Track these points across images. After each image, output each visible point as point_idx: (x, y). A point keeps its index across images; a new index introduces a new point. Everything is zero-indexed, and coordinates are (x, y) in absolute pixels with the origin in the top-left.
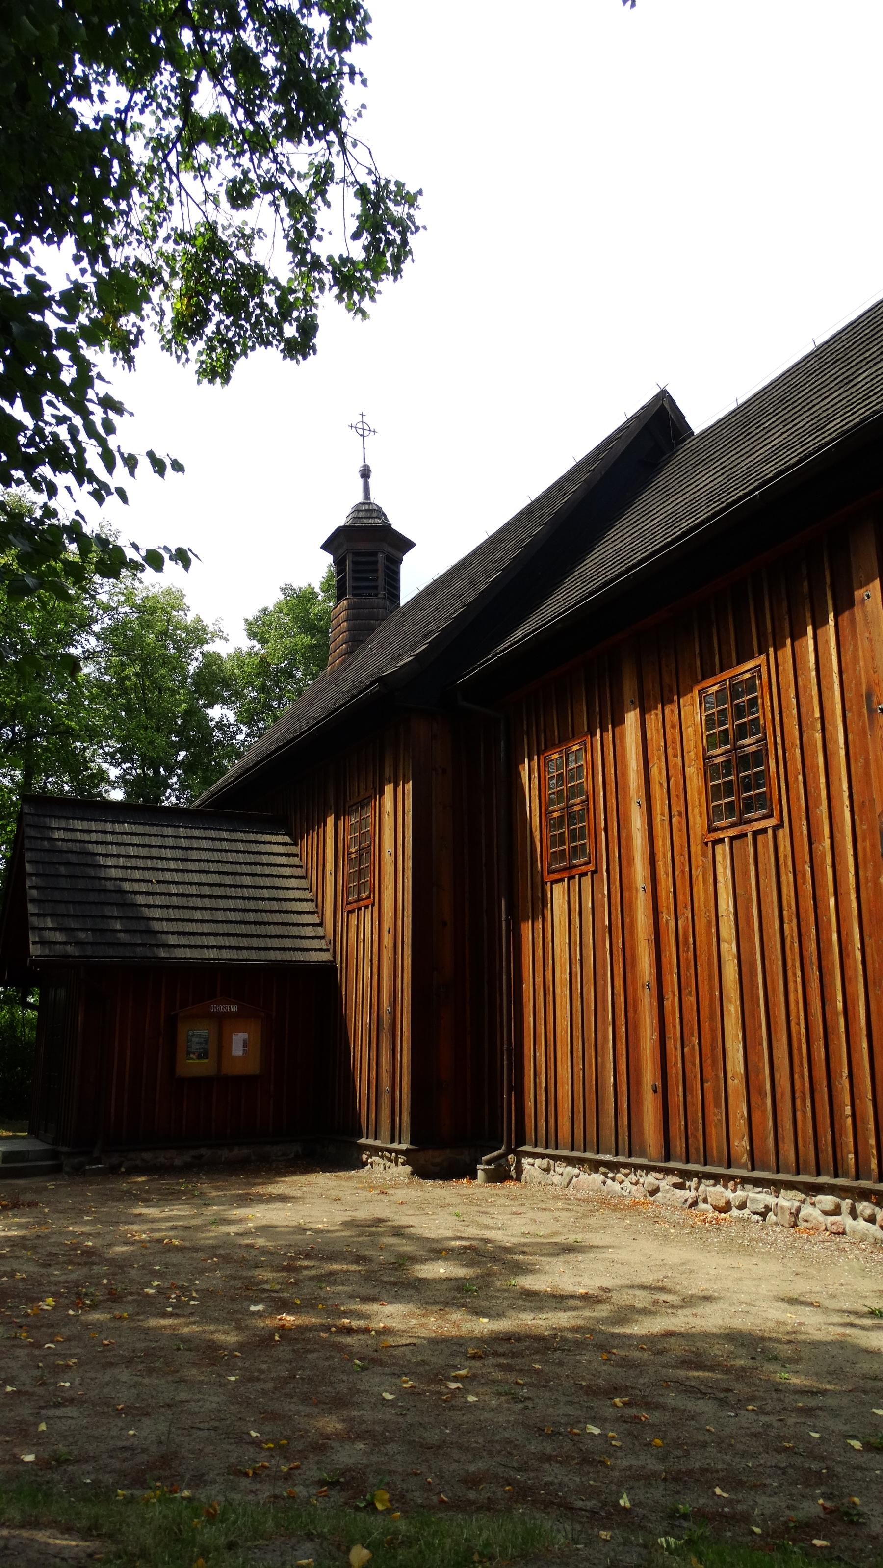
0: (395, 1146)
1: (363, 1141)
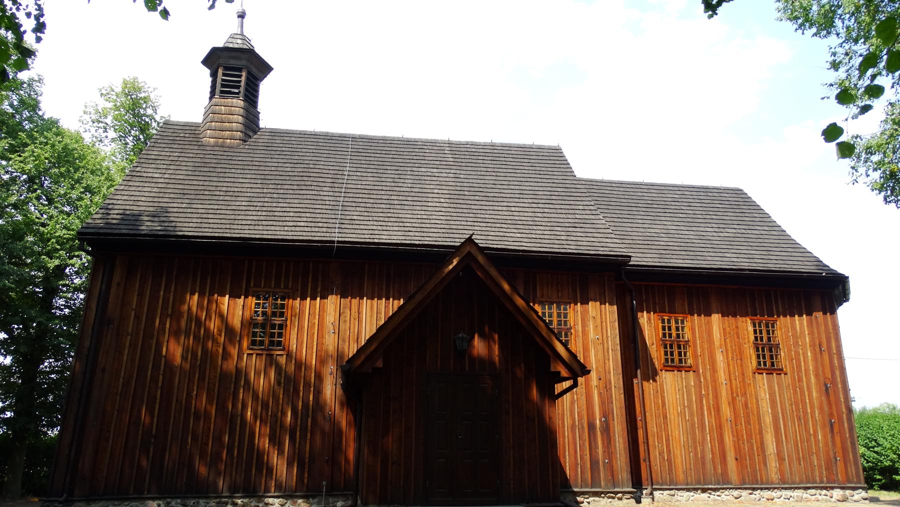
0: (616, 490)
1: (575, 490)
